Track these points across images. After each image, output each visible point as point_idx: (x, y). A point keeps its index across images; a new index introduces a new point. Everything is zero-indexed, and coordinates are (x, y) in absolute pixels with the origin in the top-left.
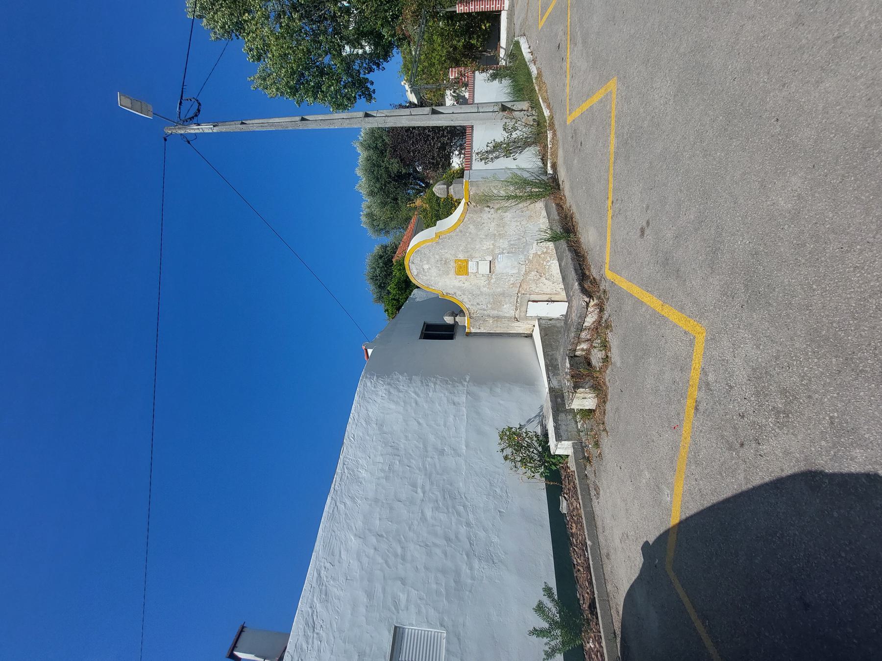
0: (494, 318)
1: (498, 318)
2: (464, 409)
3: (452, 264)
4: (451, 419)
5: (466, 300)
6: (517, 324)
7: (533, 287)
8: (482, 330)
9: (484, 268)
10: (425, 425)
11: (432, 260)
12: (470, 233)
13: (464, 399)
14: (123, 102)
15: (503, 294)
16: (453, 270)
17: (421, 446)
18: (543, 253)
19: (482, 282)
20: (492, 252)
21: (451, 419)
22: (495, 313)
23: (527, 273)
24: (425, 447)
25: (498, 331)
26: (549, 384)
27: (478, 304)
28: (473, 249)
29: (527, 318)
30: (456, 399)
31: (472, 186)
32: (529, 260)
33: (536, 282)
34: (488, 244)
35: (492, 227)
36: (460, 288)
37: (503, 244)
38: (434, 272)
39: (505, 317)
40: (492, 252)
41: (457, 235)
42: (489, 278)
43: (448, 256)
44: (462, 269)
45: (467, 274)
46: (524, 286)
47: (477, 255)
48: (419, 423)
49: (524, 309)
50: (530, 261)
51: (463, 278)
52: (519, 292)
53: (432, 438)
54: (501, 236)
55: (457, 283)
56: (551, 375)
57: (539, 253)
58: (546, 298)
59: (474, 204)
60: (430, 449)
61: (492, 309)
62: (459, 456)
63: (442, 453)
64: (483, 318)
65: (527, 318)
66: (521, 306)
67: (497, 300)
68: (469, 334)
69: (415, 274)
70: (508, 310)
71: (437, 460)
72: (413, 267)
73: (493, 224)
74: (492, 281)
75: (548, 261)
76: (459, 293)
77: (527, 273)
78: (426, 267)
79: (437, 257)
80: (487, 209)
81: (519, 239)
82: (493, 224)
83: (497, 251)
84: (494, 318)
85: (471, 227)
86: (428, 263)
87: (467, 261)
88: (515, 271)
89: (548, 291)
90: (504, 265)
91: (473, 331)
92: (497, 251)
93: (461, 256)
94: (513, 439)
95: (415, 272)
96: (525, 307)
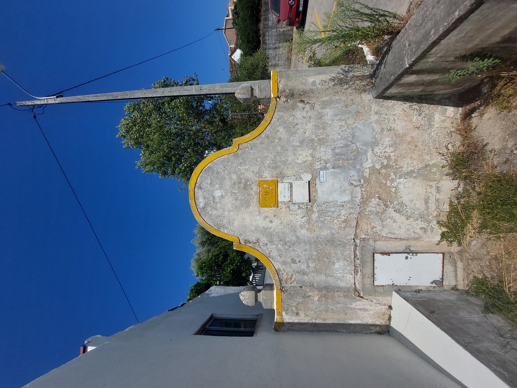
0: (320, 289)
1: (327, 291)
3: (255, 188)
5: (274, 253)
6: (359, 304)
7: (377, 224)
8: (303, 318)
9: (301, 194)
11: (228, 183)
12: (280, 139)
15: (331, 241)
18: (383, 167)
19: (298, 218)
20: (310, 168)
22: (320, 279)
23: (364, 202)
25: (331, 319)
27: (293, 261)
29: (375, 290)
31: (281, 77)
32: (364, 178)
33: (381, 215)
34: (304, 155)
35: (308, 129)
36: (265, 231)
37: (325, 153)
38: (229, 202)
39: (339, 289)
40: (310, 168)
41: (262, 143)
42: (309, 211)
43: (249, 175)
44: (269, 197)
46: (364, 226)
49: (368, 270)
50: (367, 181)
51: (269, 211)
52: (356, 235)
54: (322, 142)
55: (262, 223)
57: (378, 167)
58: (401, 246)
59: (283, 99)
61: (317, 271)
65: (375, 290)
66: (363, 263)
67: (323, 250)
68: (280, 327)
69: (201, 205)
70: (342, 274)
72: (199, 194)
74: (314, 216)
75: (392, 181)
76: (264, 240)
77: (364, 202)
78: (218, 193)
79: (234, 177)
80: (300, 105)
81: (346, 146)
82: (310, 126)
83: (318, 166)
84: (320, 289)
85: (281, 129)
86: (221, 188)
87: (276, 183)
88: (346, 198)
89: (401, 233)
90: (332, 188)
91: (287, 318)
92: (318, 166)
93: (268, 176)
95: (201, 202)
96: (370, 265)
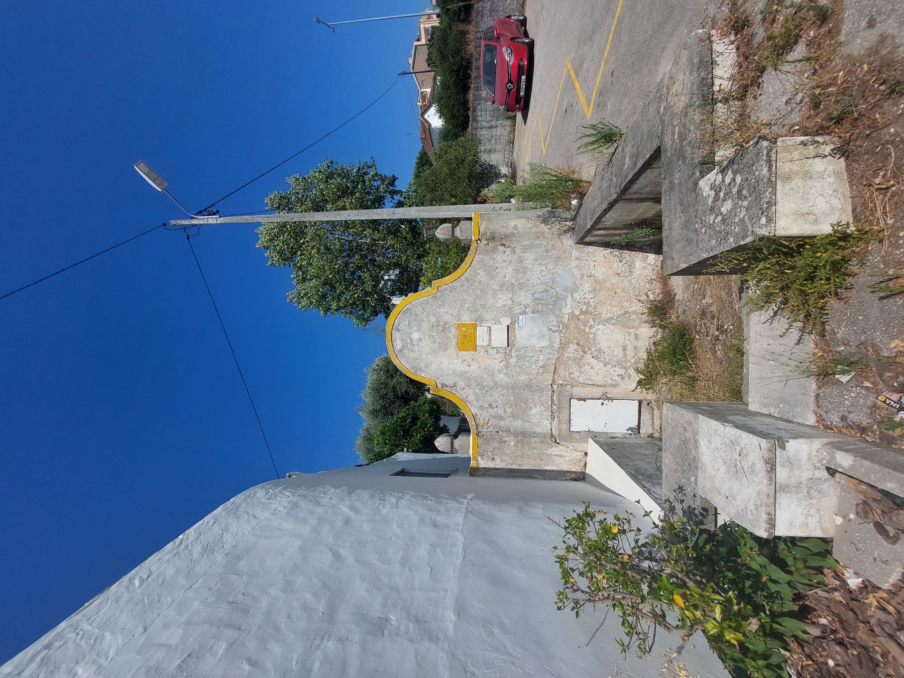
0: (516, 435)
1: (523, 436)
2: (459, 536)
3: (454, 331)
4: (423, 551)
5: (472, 398)
6: (555, 450)
7: (575, 370)
8: (498, 464)
9: (499, 338)
10: (351, 561)
11: (426, 326)
12: (480, 282)
13: (460, 519)
14: (141, 171)
15: (529, 386)
16: (454, 343)
17: (321, 607)
18: (582, 313)
19: (496, 363)
20: (509, 311)
21: (423, 551)
22: (517, 424)
23: (563, 347)
24: (331, 616)
25: (527, 465)
26: (655, 499)
27: (491, 406)
28: (483, 306)
29: (572, 436)
30: (441, 519)
31: (482, 219)
32: (563, 323)
33: (578, 361)
34: (504, 299)
35: (508, 273)
36: (462, 375)
37: (525, 298)
38: (426, 344)
39: (535, 435)
40: (509, 311)
41: (461, 286)
42: (507, 356)
43: (448, 318)
44: (467, 341)
45: (475, 348)
46: (561, 371)
47: (488, 316)
48: (337, 556)
49: (564, 417)
50: (566, 327)
51: (467, 355)
52: (553, 380)
53: (360, 590)
54: (521, 286)
55: (459, 367)
56: (648, 485)
57: (577, 313)
58: (599, 392)
59: (484, 242)
60: (344, 615)
61: (514, 416)
62: (434, 638)
63: (379, 627)
64: (498, 436)
65: (572, 436)
66: (560, 409)
67: (520, 395)
68: (475, 472)
69: (399, 348)
70: (539, 419)
71: (354, 650)
72: (397, 335)
73: (510, 269)
74: (513, 361)
75: (591, 327)
76: (461, 384)
77: (563, 347)
78: (416, 336)
79: (433, 319)
80: (501, 248)
81: (546, 291)
82: (510, 269)
83: (517, 310)
84: (516, 435)
85: (481, 272)
86: (419, 330)
87: (475, 327)
88: (545, 343)
89: (598, 379)
90: (531, 333)
91: (483, 463)
92: (517, 310)
93: (466, 319)
94: (606, 565)
95: (398, 344)
96: (566, 411)
